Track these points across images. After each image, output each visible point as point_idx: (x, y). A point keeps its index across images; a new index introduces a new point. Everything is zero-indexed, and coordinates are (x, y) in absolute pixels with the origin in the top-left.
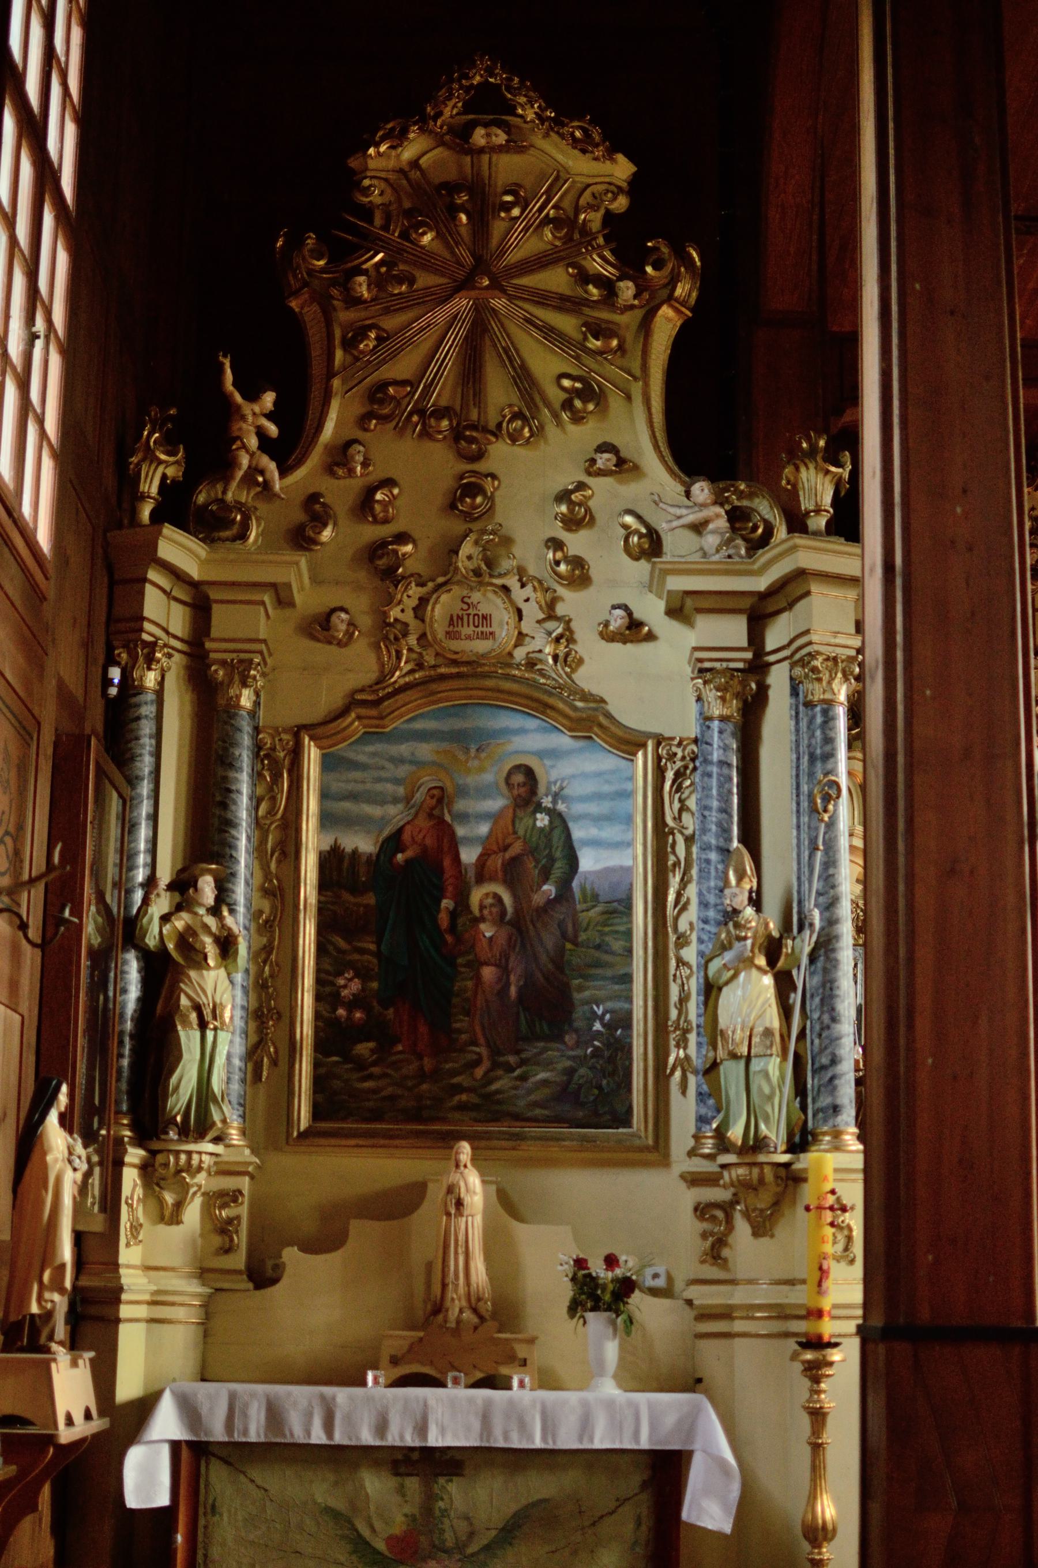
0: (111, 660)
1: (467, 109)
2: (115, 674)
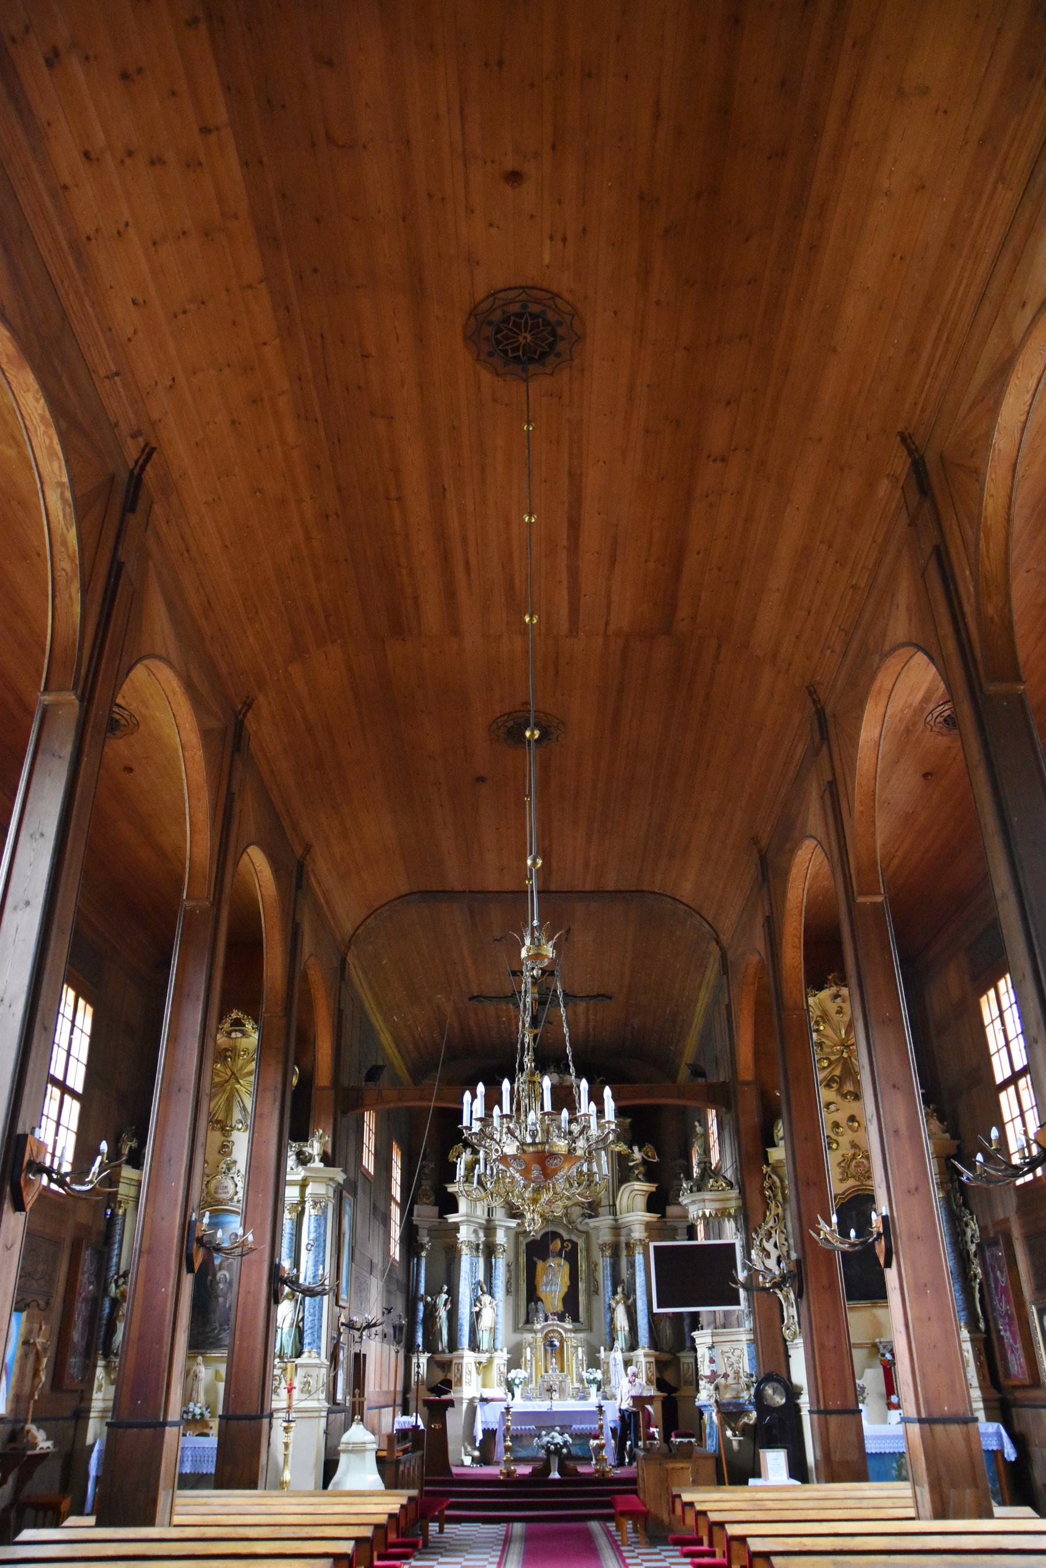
0: (109, 1207)
1: (232, 1025)
2: (109, 1212)
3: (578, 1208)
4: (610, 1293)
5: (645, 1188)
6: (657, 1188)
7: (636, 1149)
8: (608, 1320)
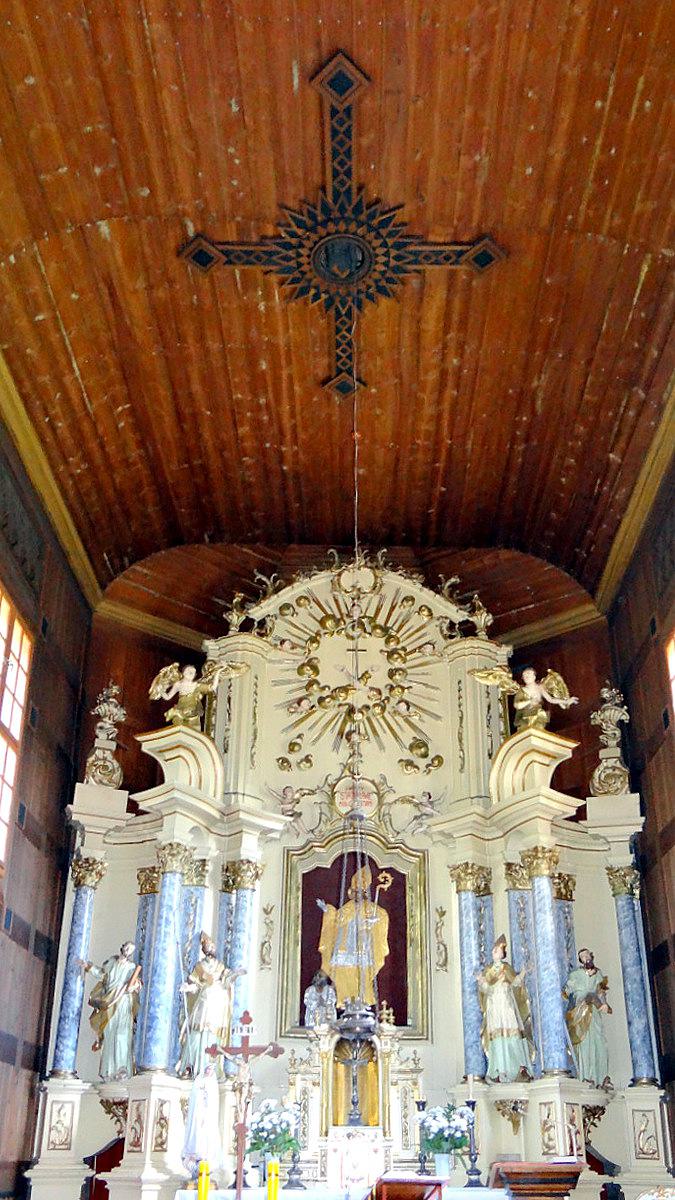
3: (409, 807)
4: (475, 963)
5: (551, 748)
6: (575, 751)
7: (529, 675)
8: (473, 1017)
